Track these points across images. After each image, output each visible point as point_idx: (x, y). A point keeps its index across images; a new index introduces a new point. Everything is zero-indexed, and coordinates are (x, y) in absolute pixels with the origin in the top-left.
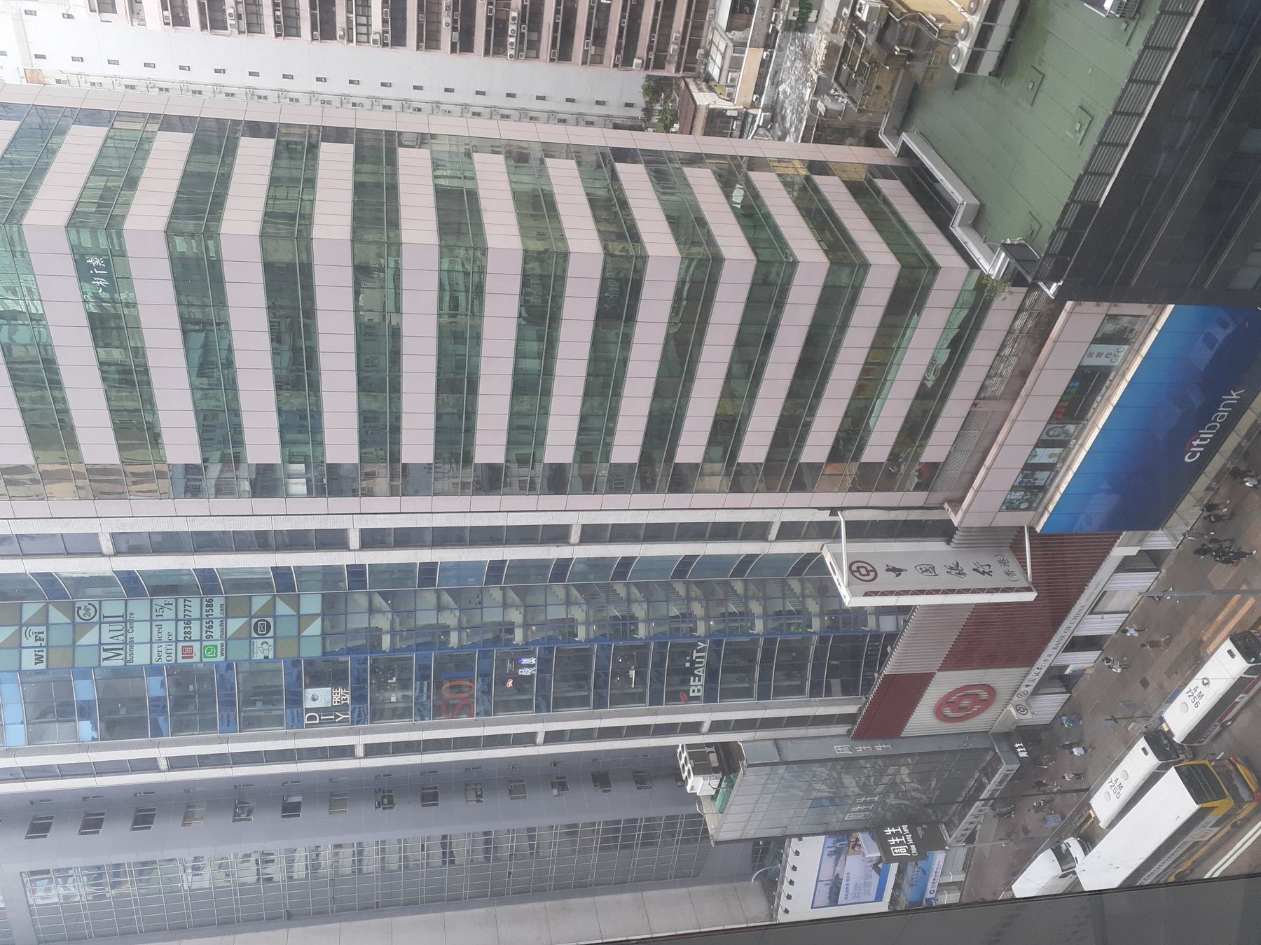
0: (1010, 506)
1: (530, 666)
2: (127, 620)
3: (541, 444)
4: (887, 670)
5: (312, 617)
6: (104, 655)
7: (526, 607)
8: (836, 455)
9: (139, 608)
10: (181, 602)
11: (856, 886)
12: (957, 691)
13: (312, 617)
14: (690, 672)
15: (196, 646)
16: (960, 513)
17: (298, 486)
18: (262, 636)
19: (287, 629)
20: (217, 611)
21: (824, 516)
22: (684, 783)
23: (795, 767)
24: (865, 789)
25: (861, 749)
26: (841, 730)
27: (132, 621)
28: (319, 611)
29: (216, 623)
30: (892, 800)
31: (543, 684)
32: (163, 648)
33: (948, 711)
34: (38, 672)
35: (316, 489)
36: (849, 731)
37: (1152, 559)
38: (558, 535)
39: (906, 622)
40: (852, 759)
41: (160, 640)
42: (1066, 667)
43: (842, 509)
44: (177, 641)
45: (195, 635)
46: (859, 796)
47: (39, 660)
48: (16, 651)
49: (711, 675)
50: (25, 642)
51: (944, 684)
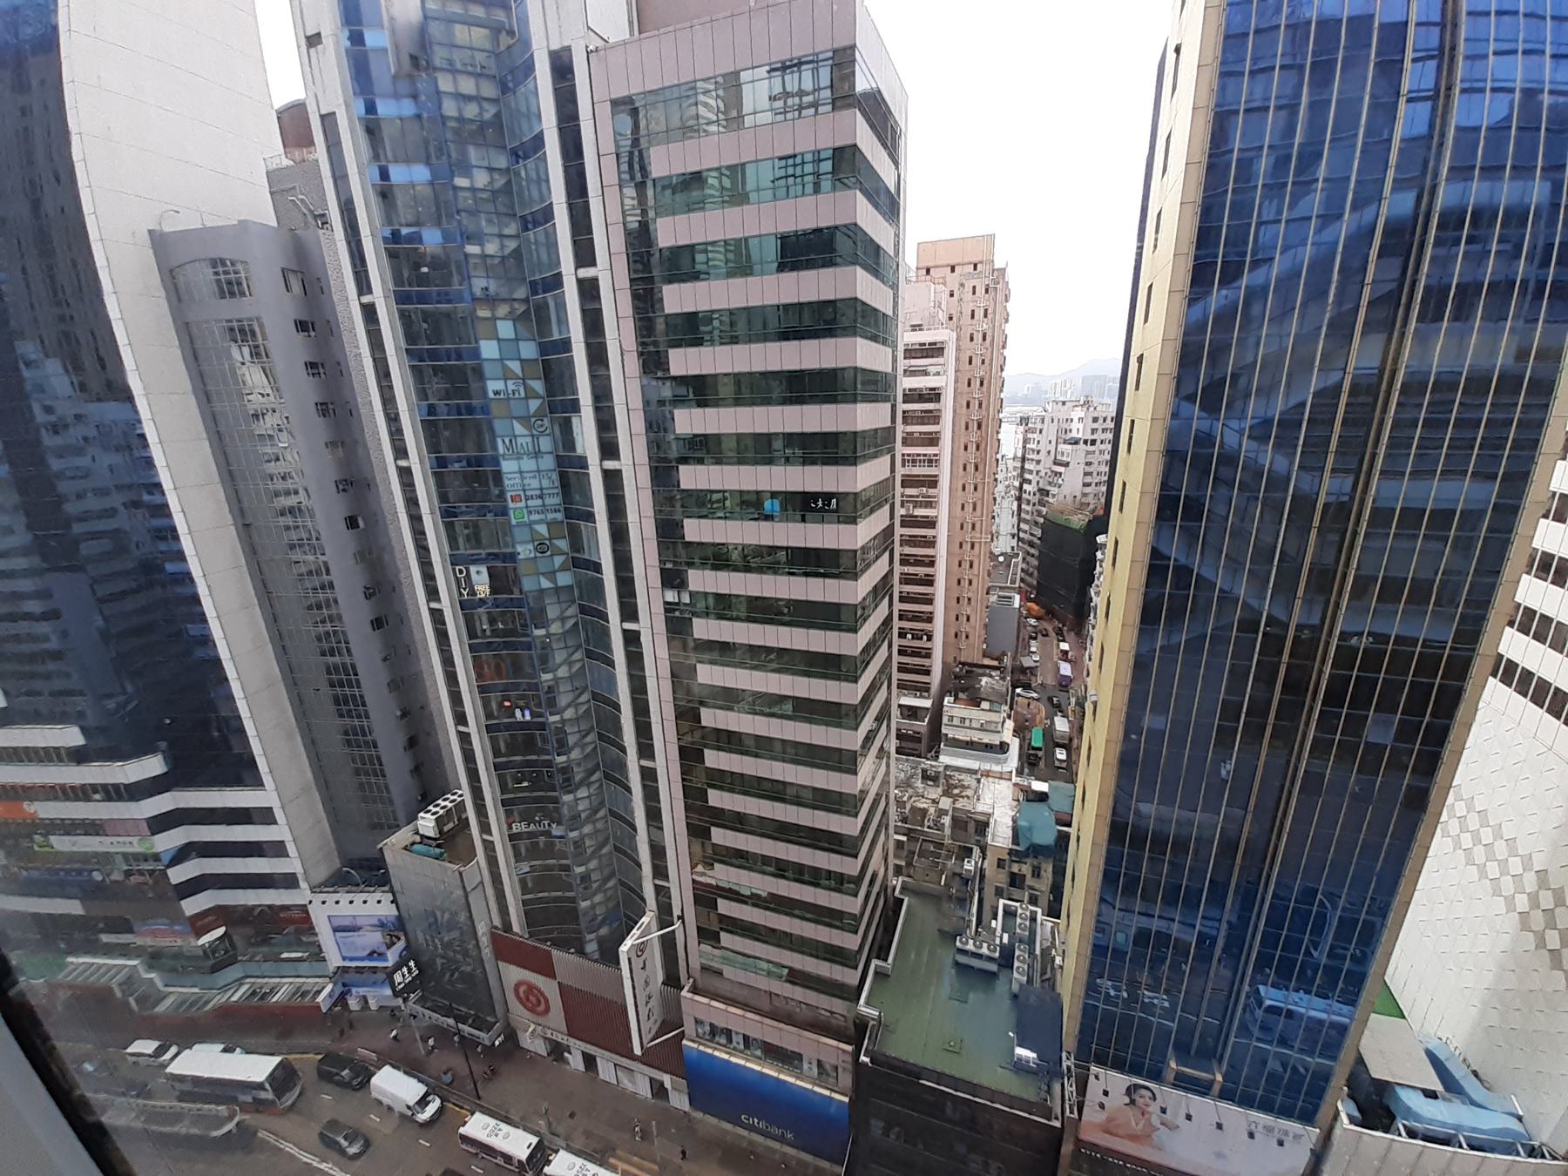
0: (698, 1022)
1: (523, 716)
2: (537, 454)
3: (719, 749)
4: (555, 953)
5: (554, 581)
6: (507, 441)
7: (577, 719)
8: (722, 918)
9: (548, 462)
10: (556, 491)
11: (353, 943)
12: (539, 991)
13: (554, 581)
14: (530, 821)
15: (523, 504)
16: (690, 995)
17: (671, 596)
18: (536, 549)
19: (543, 566)
20: (550, 516)
21: (676, 912)
22: (424, 809)
23: (463, 901)
24: (447, 946)
25: (484, 940)
26: (497, 922)
27: (536, 457)
28: (560, 584)
29: (543, 517)
30: (439, 961)
31: (508, 727)
32: (517, 481)
33: (522, 989)
34: (485, 392)
35: (669, 607)
36: (496, 928)
37: (659, 1090)
38: (646, 750)
39: (596, 961)
40: (476, 934)
41: (523, 478)
42: (570, 1053)
43: (683, 922)
44: (524, 491)
45: (530, 503)
46: (441, 940)
47: (497, 393)
48: (501, 375)
49: (531, 835)
50: (510, 383)
51: (549, 987)
